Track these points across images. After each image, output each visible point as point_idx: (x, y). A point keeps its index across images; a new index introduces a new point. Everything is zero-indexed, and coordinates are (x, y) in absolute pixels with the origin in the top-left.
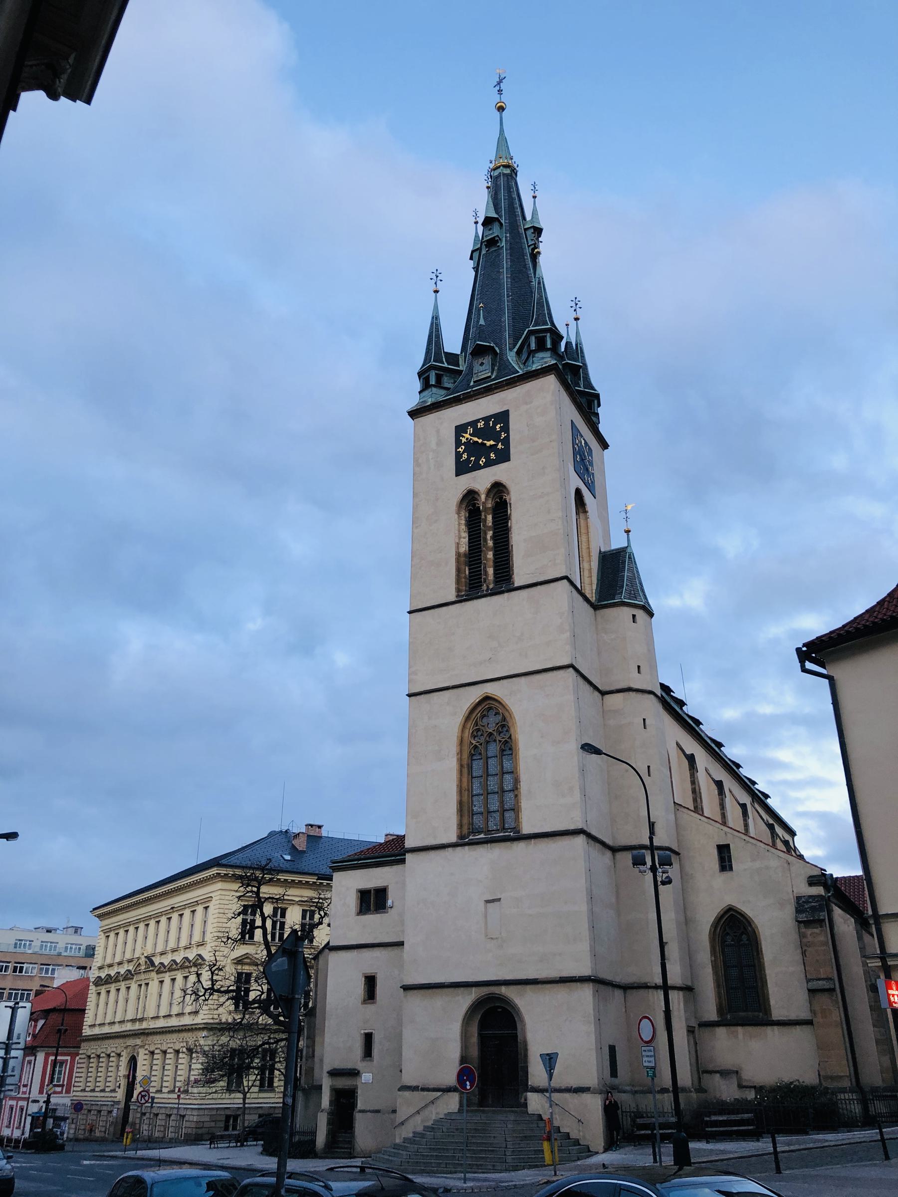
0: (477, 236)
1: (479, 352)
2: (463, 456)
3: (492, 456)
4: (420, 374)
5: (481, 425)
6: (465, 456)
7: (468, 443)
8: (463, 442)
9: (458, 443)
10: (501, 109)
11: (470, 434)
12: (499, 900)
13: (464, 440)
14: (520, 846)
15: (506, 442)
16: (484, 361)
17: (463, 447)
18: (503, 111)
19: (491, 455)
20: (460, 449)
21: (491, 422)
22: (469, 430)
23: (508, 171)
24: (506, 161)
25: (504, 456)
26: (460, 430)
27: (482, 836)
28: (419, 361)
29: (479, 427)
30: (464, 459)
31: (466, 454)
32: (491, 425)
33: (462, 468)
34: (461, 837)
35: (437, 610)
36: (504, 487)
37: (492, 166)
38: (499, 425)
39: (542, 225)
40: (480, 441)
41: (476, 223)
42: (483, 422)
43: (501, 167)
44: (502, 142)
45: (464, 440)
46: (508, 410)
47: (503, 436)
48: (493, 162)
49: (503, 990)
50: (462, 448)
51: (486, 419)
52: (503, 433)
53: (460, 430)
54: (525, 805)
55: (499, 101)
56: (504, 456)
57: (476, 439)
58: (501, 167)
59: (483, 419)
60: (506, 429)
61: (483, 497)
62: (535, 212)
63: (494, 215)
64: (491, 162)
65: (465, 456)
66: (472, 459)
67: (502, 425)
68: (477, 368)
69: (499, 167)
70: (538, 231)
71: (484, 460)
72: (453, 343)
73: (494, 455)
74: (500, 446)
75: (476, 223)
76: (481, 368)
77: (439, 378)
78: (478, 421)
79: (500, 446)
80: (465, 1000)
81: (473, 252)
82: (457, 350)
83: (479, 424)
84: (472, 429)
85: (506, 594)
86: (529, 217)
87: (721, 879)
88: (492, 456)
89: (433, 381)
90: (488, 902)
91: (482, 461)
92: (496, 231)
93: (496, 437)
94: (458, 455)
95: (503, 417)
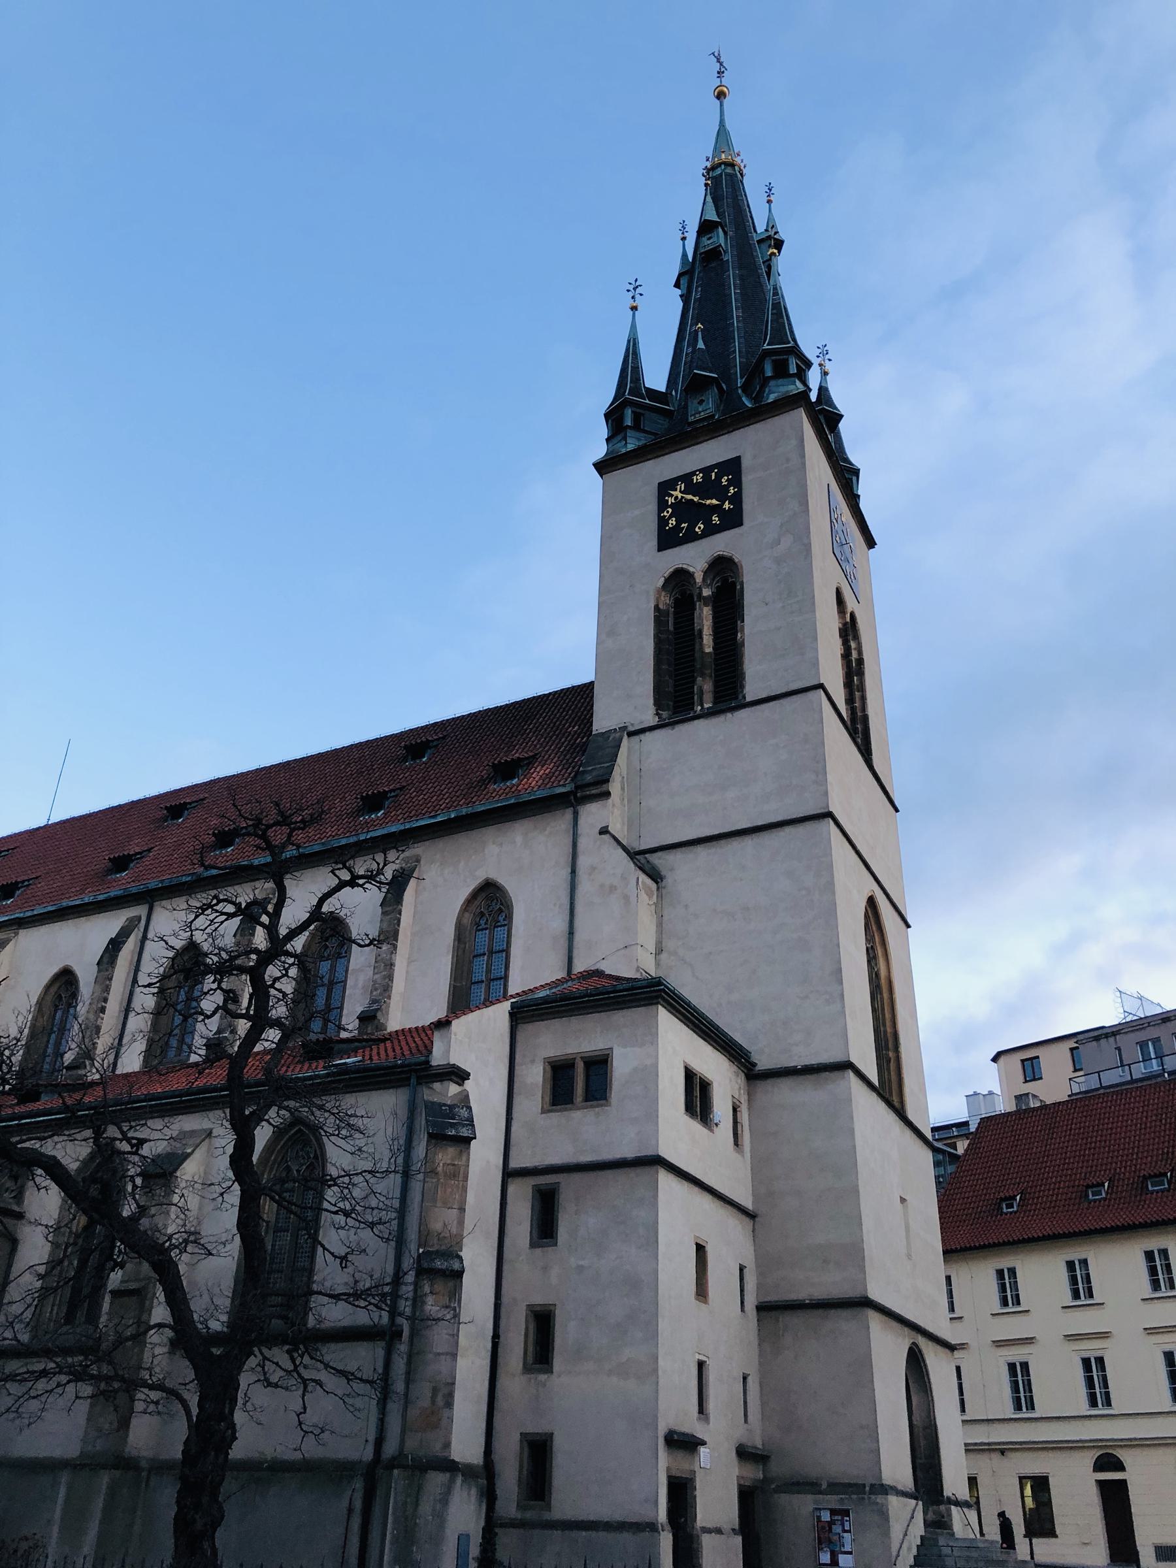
0: (685, 255)
1: (696, 386)
2: (670, 522)
3: (715, 519)
4: (608, 416)
5: (698, 478)
6: (673, 522)
7: (679, 504)
8: (670, 503)
9: (662, 505)
10: (720, 96)
11: (681, 492)
13: (671, 500)
15: (737, 500)
16: (703, 398)
17: (670, 510)
18: (725, 96)
19: (713, 518)
20: (665, 513)
21: (713, 474)
22: (678, 487)
23: (729, 170)
24: (730, 157)
25: (733, 519)
26: (665, 487)
28: (606, 396)
29: (695, 481)
30: (670, 525)
31: (674, 519)
32: (713, 478)
33: (667, 540)
36: (735, 563)
37: (709, 165)
38: (726, 478)
39: (782, 235)
40: (696, 499)
41: (684, 239)
42: (701, 475)
43: (723, 167)
44: (722, 134)
45: (671, 500)
46: (739, 457)
47: (732, 491)
48: (710, 159)
50: (668, 512)
51: (706, 471)
52: (732, 488)
55: (719, 84)
56: (733, 519)
57: (689, 497)
58: (723, 167)
59: (701, 471)
60: (737, 482)
61: (699, 578)
62: (770, 219)
63: (712, 216)
64: (708, 160)
66: (683, 525)
67: (730, 477)
68: (693, 405)
70: (779, 244)
71: (702, 526)
72: (656, 376)
73: (717, 519)
74: (727, 506)
75: (684, 239)
77: (637, 418)
78: (693, 473)
79: (727, 506)
81: (680, 275)
82: (661, 386)
83: (695, 477)
84: (683, 485)
86: (761, 227)
88: (715, 519)
91: (699, 528)
92: (719, 238)
93: (722, 495)
94: (662, 522)
95: (733, 467)
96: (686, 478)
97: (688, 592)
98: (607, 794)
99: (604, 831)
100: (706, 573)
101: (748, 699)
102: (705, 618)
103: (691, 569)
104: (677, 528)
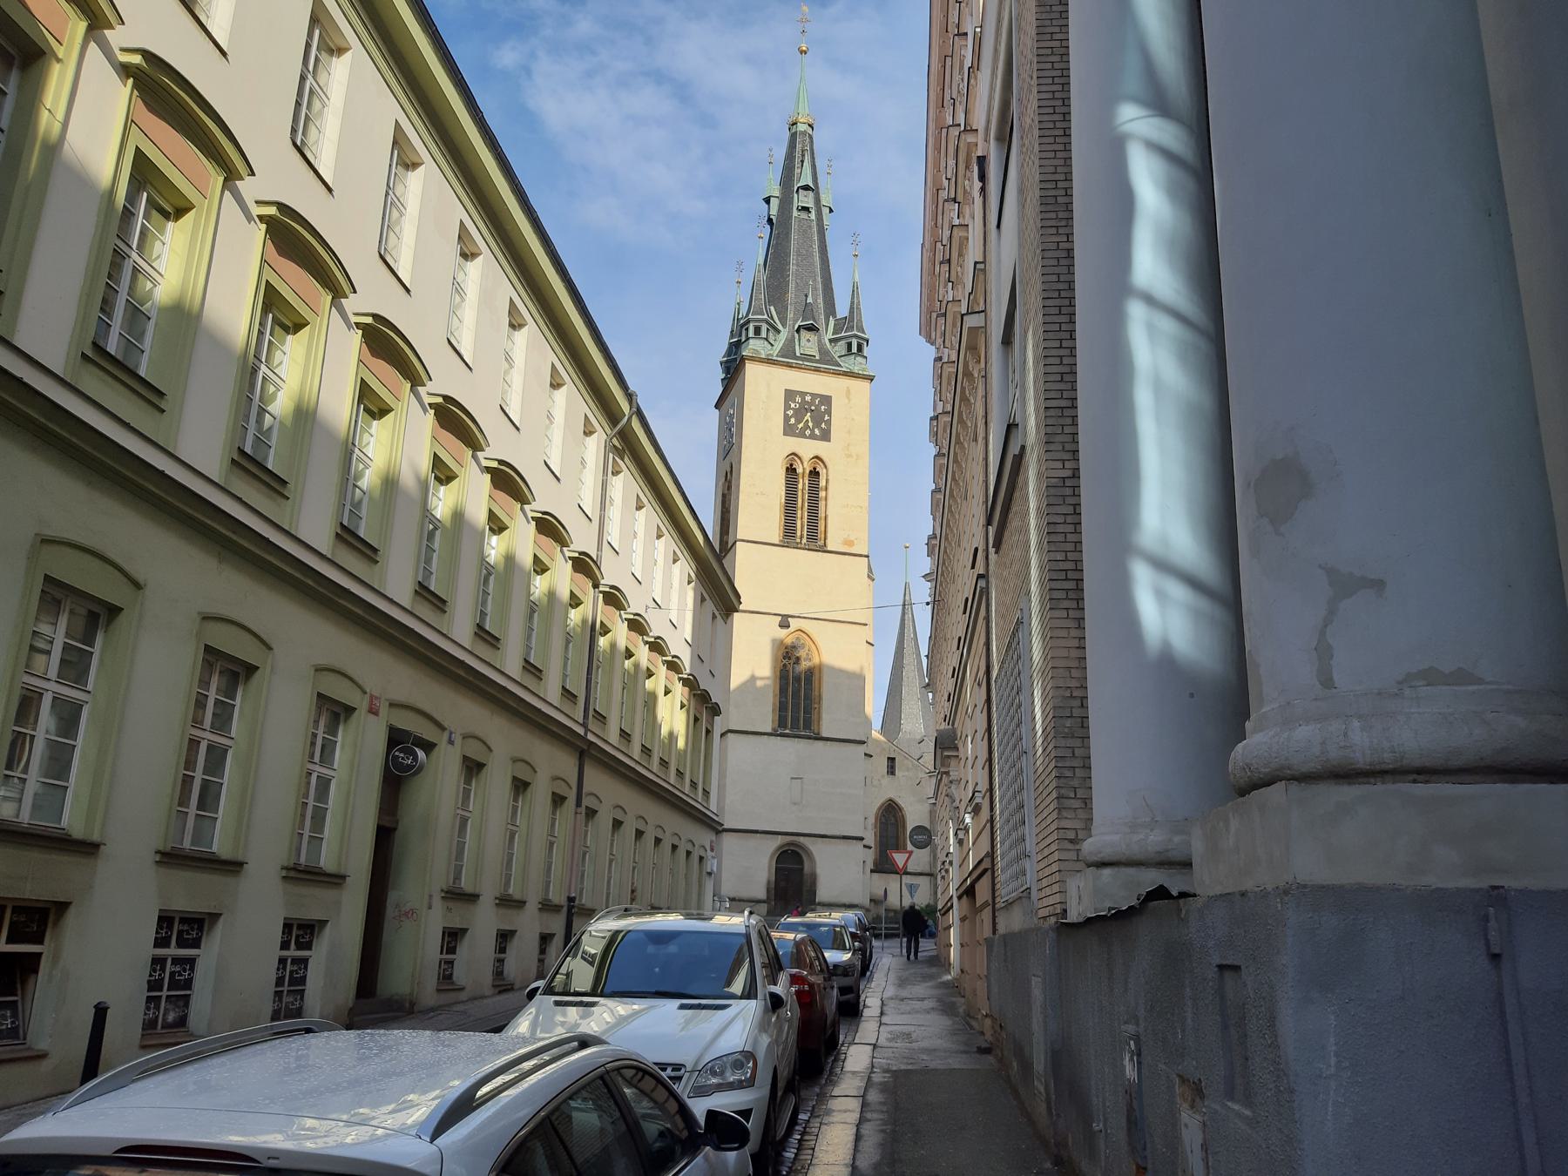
3: (817, 432)
5: (808, 398)
6: (793, 421)
9: (787, 407)
12: (801, 778)
13: (793, 405)
14: (820, 744)
15: (829, 423)
20: (788, 412)
25: (826, 436)
26: (790, 395)
27: (787, 731)
33: (789, 430)
34: (774, 729)
35: (760, 545)
49: (802, 839)
51: (814, 396)
53: (790, 395)
54: (825, 717)
56: (826, 436)
59: (811, 394)
65: (793, 421)
74: (823, 426)
76: (808, 344)
80: (774, 843)
85: (820, 553)
87: (887, 780)
90: (792, 778)
94: (787, 418)
95: (827, 400)
96: (803, 394)
97: (794, 466)
102: (803, 484)
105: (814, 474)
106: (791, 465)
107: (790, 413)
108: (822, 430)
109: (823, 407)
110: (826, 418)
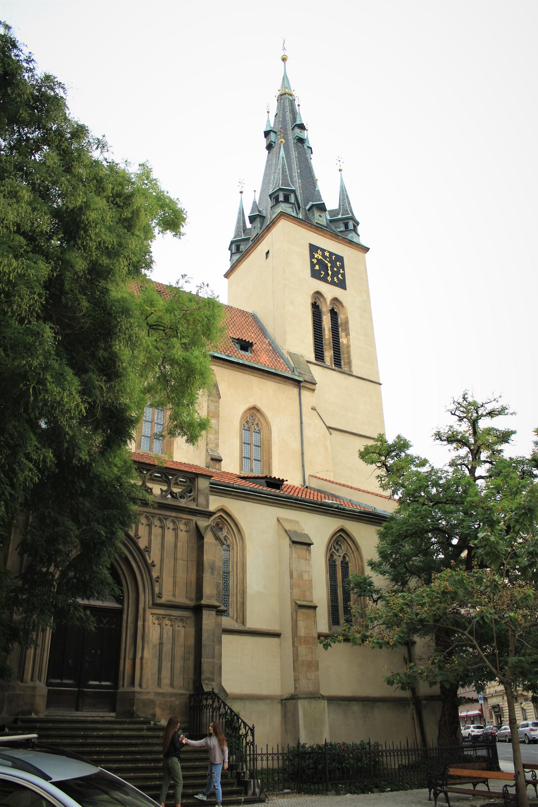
0: (268, 121)
3: (336, 280)
5: (327, 254)
6: (317, 267)
9: (312, 257)
10: (284, 60)
13: (316, 256)
15: (343, 275)
25: (342, 285)
26: (313, 249)
33: (315, 274)
36: (343, 306)
44: (285, 78)
51: (331, 254)
56: (342, 285)
59: (328, 252)
60: (342, 267)
65: (317, 267)
69: (285, 94)
74: (340, 276)
78: (325, 250)
89: (281, 198)
94: (313, 265)
95: (340, 259)
96: (323, 251)
98: (313, 390)
99: (313, 409)
100: (331, 301)
101: (354, 374)
103: (325, 296)
104: (319, 271)
105: (334, 314)
106: (315, 303)
107: (315, 261)
108: (338, 278)
109: (338, 263)
110: (341, 272)
